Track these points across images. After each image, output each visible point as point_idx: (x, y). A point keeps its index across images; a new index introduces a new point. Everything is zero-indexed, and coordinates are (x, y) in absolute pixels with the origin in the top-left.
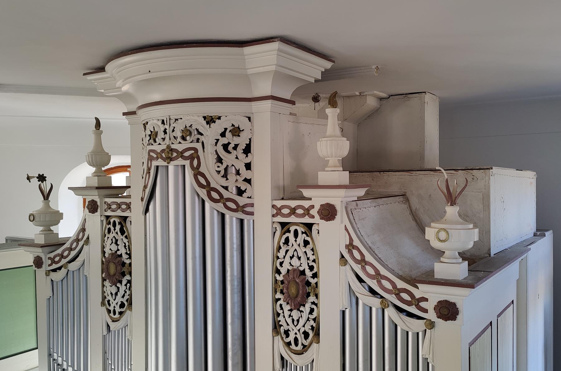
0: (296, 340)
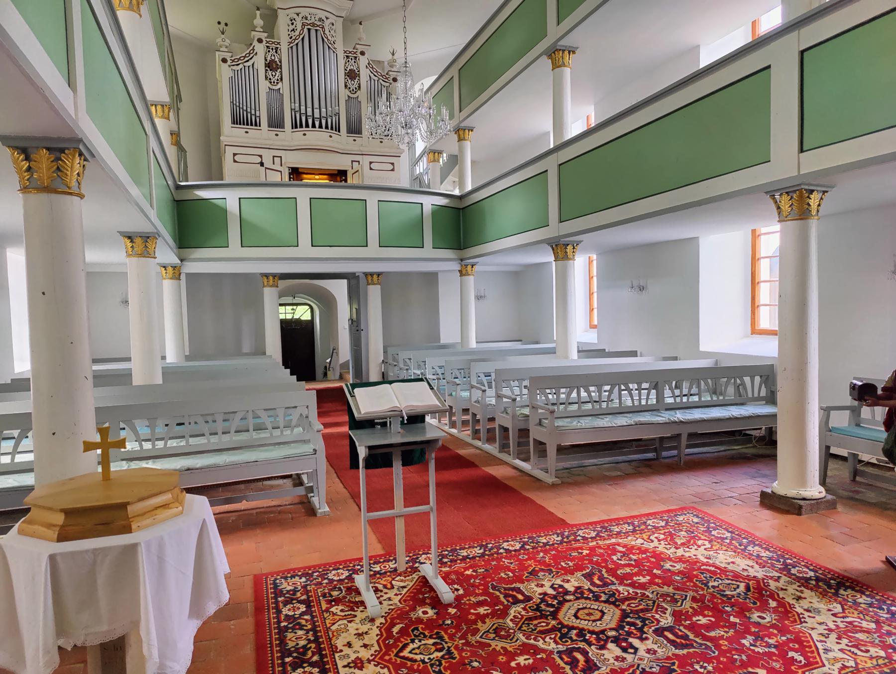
0: (353, 90)
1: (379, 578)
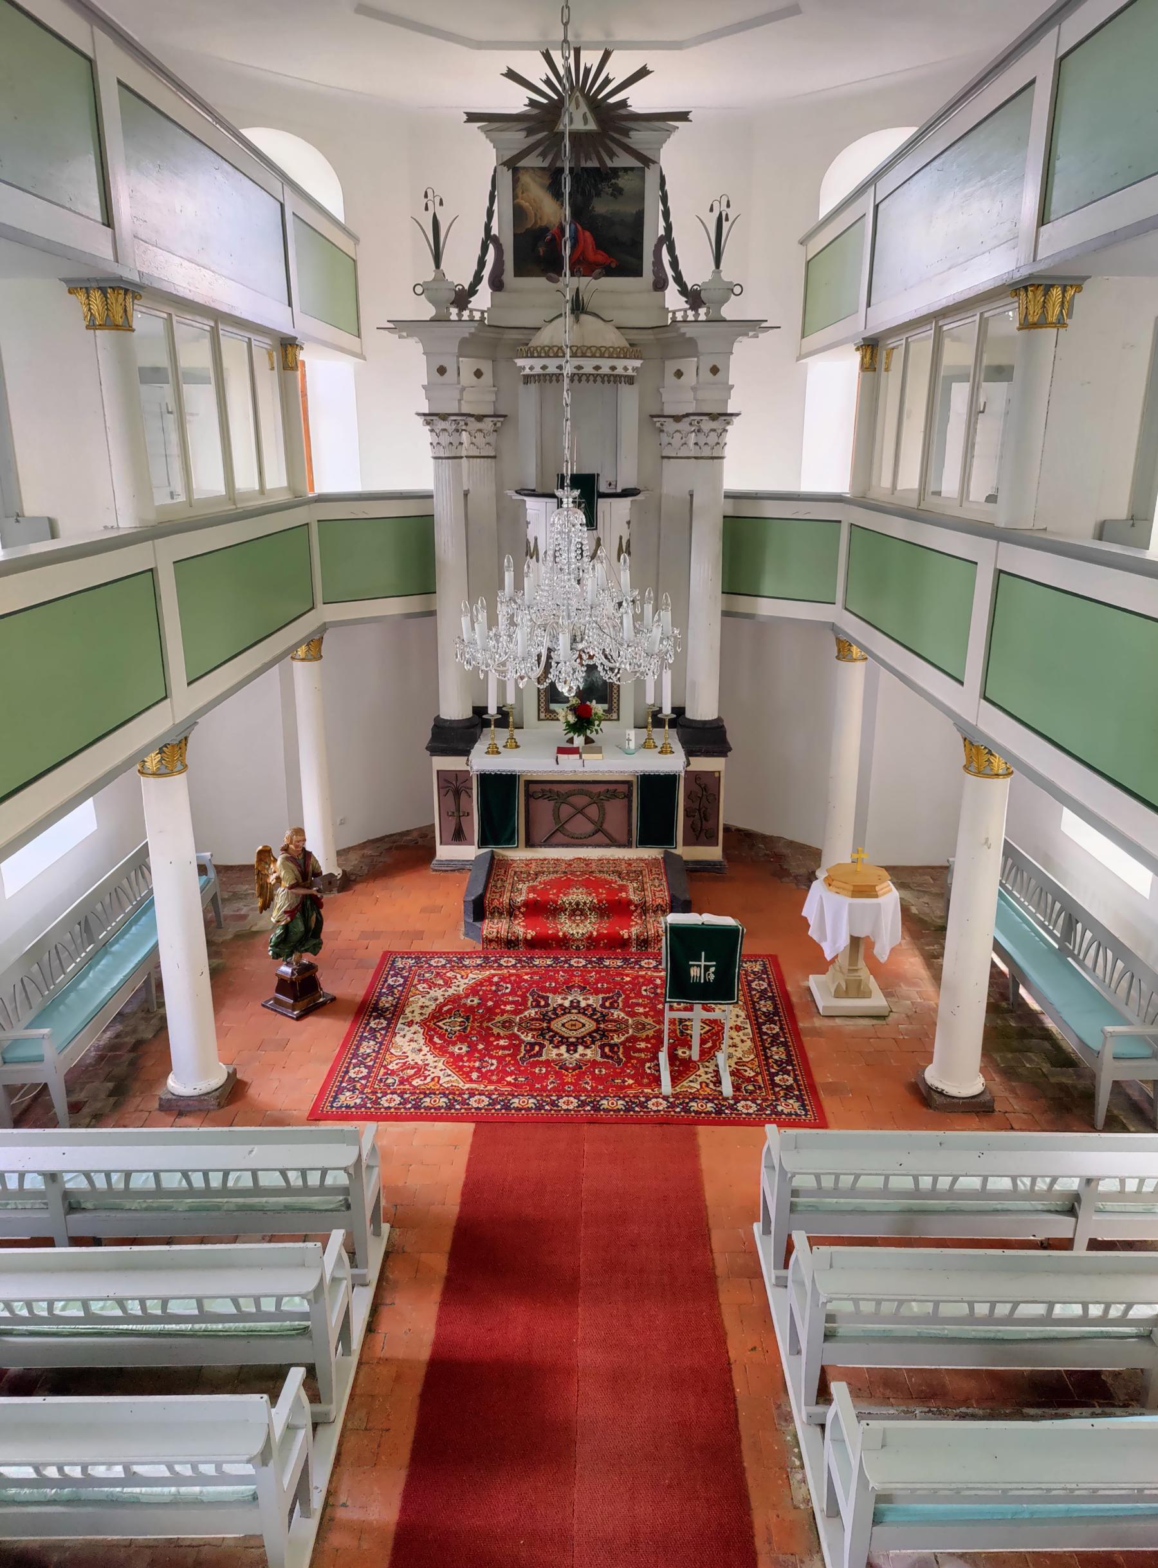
1: (710, 1095)
